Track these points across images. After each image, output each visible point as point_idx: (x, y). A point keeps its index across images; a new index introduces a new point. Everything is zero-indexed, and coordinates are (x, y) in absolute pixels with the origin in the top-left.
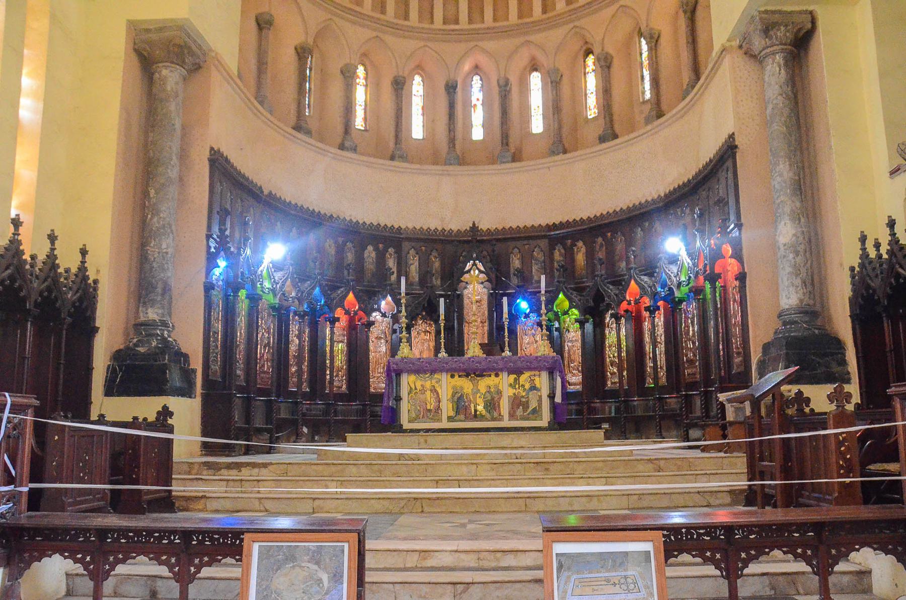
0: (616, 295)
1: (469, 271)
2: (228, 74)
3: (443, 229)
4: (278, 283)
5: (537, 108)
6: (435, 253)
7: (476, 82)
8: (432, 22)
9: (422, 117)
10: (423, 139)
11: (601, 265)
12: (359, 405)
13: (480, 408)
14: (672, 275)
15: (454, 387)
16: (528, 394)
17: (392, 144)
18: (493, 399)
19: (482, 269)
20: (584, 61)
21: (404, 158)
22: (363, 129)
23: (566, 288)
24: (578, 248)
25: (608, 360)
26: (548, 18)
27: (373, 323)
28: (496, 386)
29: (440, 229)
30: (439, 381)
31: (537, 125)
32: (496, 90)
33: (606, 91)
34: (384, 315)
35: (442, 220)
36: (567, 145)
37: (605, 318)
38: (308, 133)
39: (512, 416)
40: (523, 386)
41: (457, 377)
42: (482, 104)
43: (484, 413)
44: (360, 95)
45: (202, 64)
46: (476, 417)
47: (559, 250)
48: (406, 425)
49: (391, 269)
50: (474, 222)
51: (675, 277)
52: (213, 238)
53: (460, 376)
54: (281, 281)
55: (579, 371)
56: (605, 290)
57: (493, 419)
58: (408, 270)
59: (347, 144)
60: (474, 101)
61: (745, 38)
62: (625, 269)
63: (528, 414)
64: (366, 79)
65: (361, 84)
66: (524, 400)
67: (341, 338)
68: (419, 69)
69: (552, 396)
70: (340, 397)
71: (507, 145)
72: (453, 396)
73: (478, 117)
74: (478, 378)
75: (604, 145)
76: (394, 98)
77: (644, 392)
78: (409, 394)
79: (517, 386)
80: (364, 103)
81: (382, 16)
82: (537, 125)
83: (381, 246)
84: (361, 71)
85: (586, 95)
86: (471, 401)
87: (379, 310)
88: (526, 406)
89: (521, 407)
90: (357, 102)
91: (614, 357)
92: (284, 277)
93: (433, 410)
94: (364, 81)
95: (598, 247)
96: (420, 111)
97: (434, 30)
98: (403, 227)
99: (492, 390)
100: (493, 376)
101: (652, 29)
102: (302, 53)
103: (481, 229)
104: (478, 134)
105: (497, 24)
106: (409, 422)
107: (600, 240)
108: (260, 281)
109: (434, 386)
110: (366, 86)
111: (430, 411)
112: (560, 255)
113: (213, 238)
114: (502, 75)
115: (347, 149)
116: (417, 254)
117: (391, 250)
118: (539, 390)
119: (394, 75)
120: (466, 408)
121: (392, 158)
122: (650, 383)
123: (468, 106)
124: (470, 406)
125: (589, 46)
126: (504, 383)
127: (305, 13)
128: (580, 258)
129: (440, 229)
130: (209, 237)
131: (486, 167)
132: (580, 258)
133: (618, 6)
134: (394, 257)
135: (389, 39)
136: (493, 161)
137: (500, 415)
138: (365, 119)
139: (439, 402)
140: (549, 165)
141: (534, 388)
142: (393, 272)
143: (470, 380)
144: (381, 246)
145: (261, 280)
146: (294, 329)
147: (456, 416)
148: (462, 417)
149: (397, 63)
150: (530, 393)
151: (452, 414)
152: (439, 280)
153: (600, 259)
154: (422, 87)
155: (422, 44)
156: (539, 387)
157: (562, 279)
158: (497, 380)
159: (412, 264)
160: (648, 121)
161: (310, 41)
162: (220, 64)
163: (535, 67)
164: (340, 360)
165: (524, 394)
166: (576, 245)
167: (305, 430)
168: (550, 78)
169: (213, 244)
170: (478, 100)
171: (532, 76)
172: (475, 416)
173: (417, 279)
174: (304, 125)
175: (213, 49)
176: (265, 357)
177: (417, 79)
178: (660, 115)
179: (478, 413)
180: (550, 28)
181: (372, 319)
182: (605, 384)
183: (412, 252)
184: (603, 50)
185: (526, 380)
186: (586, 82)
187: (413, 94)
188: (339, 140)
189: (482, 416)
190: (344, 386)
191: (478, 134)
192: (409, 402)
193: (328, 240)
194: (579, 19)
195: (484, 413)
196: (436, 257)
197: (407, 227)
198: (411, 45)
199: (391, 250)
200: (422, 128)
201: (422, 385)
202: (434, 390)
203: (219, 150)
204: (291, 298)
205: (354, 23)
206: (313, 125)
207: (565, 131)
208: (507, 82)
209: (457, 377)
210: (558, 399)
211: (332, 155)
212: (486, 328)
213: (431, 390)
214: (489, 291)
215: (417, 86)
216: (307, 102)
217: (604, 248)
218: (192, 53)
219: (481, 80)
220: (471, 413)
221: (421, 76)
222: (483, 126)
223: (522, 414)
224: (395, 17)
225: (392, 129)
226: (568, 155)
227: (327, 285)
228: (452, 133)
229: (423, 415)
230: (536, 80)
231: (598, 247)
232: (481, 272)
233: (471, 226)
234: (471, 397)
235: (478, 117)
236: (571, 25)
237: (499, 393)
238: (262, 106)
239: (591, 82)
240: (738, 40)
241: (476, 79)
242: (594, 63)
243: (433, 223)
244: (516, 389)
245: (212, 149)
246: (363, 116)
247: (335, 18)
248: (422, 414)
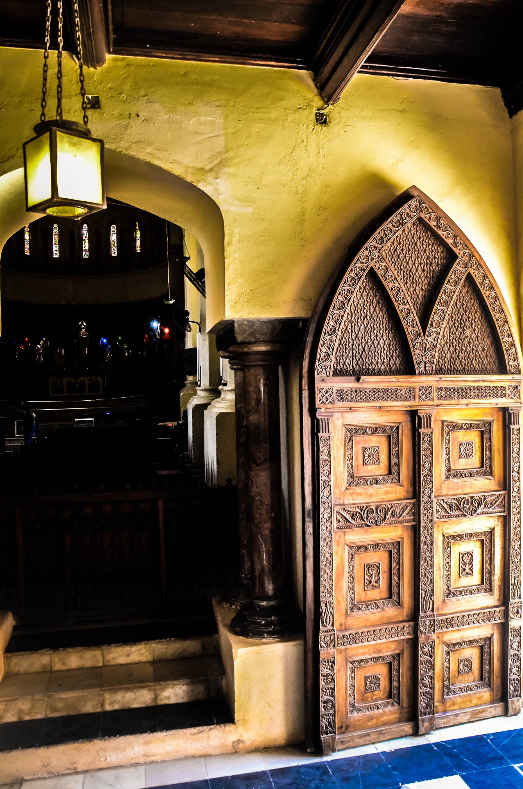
126: (86, 379)
170: (86, 237)
177: (55, 226)
187: (53, 233)
210: (105, 384)
241: (85, 225)
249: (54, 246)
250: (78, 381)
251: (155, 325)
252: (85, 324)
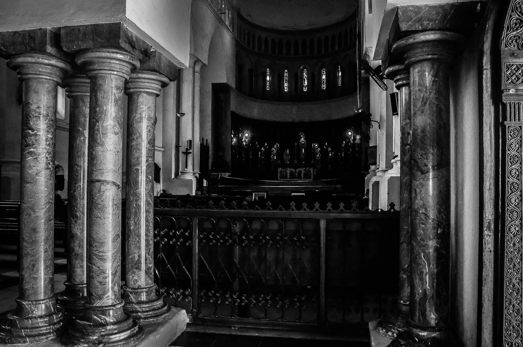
30: (287, 169)
34: (275, 149)
48: (279, 179)
64: (270, 73)
69: (313, 173)
85: (338, 78)
87: (274, 147)
126: (303, 170)
170: (305, 77)
202: (286, 171)
210: (315, 173)
232: (303, 136)
249: (285, 84)
250: (297, 171)
251: (350, 133)
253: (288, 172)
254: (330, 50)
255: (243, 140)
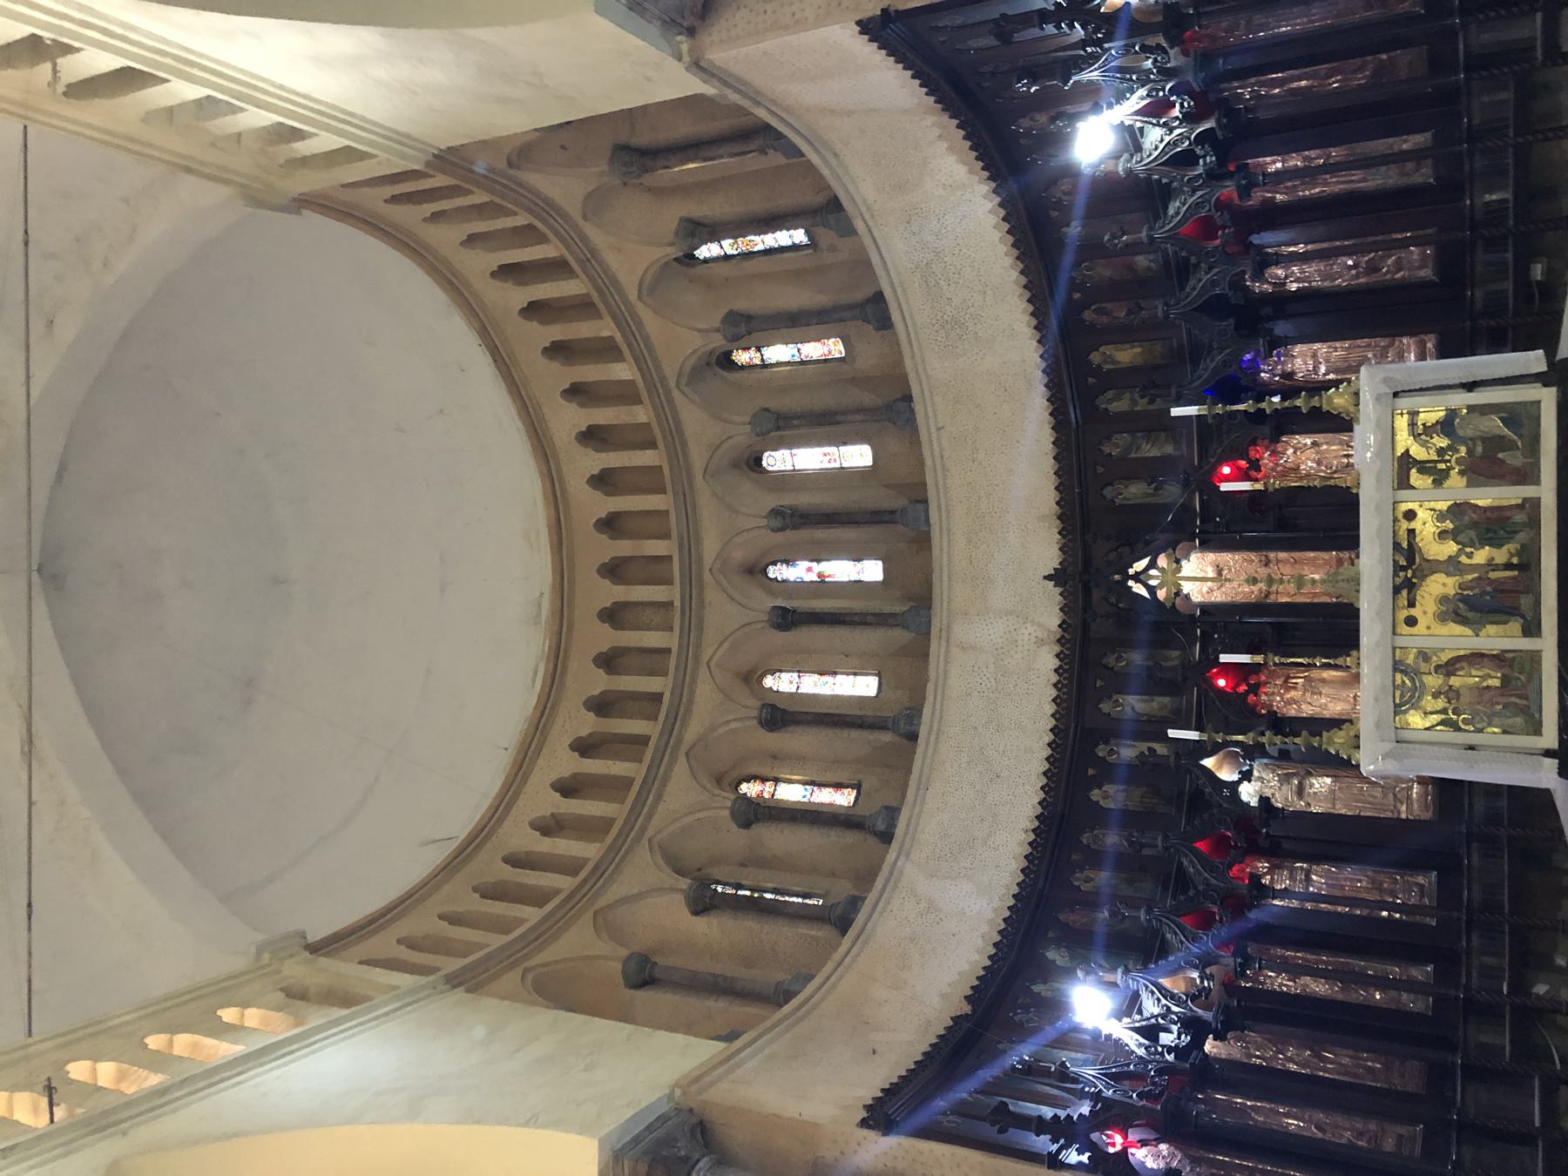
0: (1210, 268)
1: (1151, 590)
2: (721, 1063)
3: (1059, 641)
4: (1168, 1008)
5: (828, 457)
6: (1110, 660)
7: (778, 572)
8: (668, 651)
9: (838, 677)
10: (879, 675)
11: (1141, 309)
12: (1468, 849)
13: (1501, 556)
14: (1167, 139)
15: (1442, 618)
16: (1463, 441)
17: (886, 737)
18: (1474, 525)
19: (1144, 563)
20: (743, 367)
21: (913, 713)
22: (855, 791)
23: (1193, 381)
24: (1106, 362)
25: (1362, 280)
26: (664, 437)
27: (1264, 801)
28: (1441, 517)
29: (1057, 648)
31: (858, 456)
32: (792, 535)
33: (795, 324)
34: (1247, 776)
35: (1040, 642)
36: (899, 396)
37: (1263, 294)
38: (854, 903)
39: (1528, 475)
40: (1441, 451)
41: (1413, 612)
42: (818, 561)
43: (1512, 547)
44: (791, 793)
45: (694, 1120)
46: (1527, 565)
47: (1110, 401)
49: (1142, 753)
50: (1045, 578)
51: (1171, 130)
52: (1059, 1151)
53: (1412, 604)
54: (1164, 1001)
55: (1391, 345)
56: (1200, 295)
57: (1534, 523)
58: (1145, 718)
59: (881, 826)
60: (813, 577)
61: (673, 21)
62: (1152, 257)
63: (1520, 436)
64: (764, 780)
65: (772, 790)
66: (1479, 449)
67: (1300, 876)
68: (752, 679)
70: (1447, 894)
71: (893, 512)
72: (1462, 620)
73: (841, 570)
74: (1417, 560)
75: (895, 317)
76: (799, 729)
77: (1450, 188)
78: (1460, 729)
79: (1442, 466)
80: (808, 787)
81: (652, 744)
82: (858, 456)
83: (1091, 772)
84: (750, 789)
85: (802, 363)
86: (1479, 578)
88: (1495, 443)
89: (1500, 455)
90: (806, 800)
91: (1355, 266)
92: (1153, 993)
93: (1506, 671)
94: (768, 784)
95: (1105, 319)
96: (826, 678)
97: (680, 646)
98: (1052, 722)
99: (1451, 526)
100: (1414, 525)
101: (677, 234)
102: (703, 902)
103: (1060, 564)
104: (872, 571)
105: (674, 534)
106: (1537, 730)
107: (1088, 315)
108: (1162, 1053)
109: (1438, 667)
110: (776, 780)
111: (1505, 680)
112: (1120, 399)
113: (1059, 1151)
114: (765, 522)
115: (892, 825)
116: (1110, 697)
117: (1101, 751)
118: (1452, 414)
119: (758, 726)
120: (1500, 588)
121: (913, 737)
122: (1424, 175)
123: (822, 586)
124: (1496, 580)
125: (713, 361)
127: (635, 891)
128: (1126, 355)
129: (1057, 648)
130: (1054, 1162)
131: (936, 552)
132: (1126, 355)
133: (639, 303)
134: (1117, 745)
135: (693, 730)
136: (923, 541)
137: (1520, 507)
138: (838, 786)
139: (1482, 655)
140: (933, 430)
141: (1446, 426)
142: (1150, 749)
143: (1424, 577)
144: (1091, 772)
145: (1160, 1049)
146: (1279, 982)
147: (1523, 617)
148: (1525, 601)
149: (735, 720)
150: (1461, 433)
151: (1515, 626)
152: (1166, 652)
153: (1130, 312)
154: (783, 675)
155: (703, 671)
156: (1442, 414)
157: (1173, 391)
158: (1422, 514)
159: (1133, 708)
160: (848, 230)
161: (684, 883)
162: (696, 1079)
163: (752, 462)
164: (1356, 880)
165: (1463, 451)
166: (1099, 367)
167: (1541, 989)
168: (769, 432)
169: (1073, 1157)
170: (809, 570)
171: (770, 469)
172: (1520, 567)
173: (1167, 700)
174: (839, 911)
175: (667, 1091)
176: (1346, 1061)
177: (769, 682)
178: (835, 205)
179: (1515, 560)
180: (681, 432)
181: (1254, 802)
182: (1424, 285)
183: (1105, 707)
184: (718, 330)
185: (1424, 444)
186: (779, 364)
187: (794, 690)
188: (872, 842)
189: (1519, 553)
190: (1421, 880)
191: (872, 571)
192: (1480, 731)
193: (1076, 883)
194: (663, 379)
195: (1512, 547)
196: (1119, 659)
197: (1053, 716)
198: (705, 693)
199: (1101, 751)
200: (858, 678)
201: (1436, 696)
202: (1449, 668)
203: (868, 1108)
204: (1202, 982)
205: (659, 797)
206: (843, 889)
207: (868, 399)
208: (776, 513)
209: (1413, 612)
211: (902, 859)
212: (1282, 555)
213: (1449, 674)
214: (1195, 548)
215: (782, 683)
216: (800, 900)
217: (1104, 305)
218: (669, 1141)
219: (774, 563)
220: (1514, 578)
221: (763, 675)
222: (859, 560)
223: (1519, 454)
224: (656, 718)
225: (855, 734)
226: (915, 392)
227: (1174, 897)
228: (870, 619)
229: (1520, 697)
230: (778, 460)
231: (1105, 319)
232: (1152, 565)
233: (1053, 583)
234: (1470, 577)
235: (841, 570)
236: (676, 393)
237: (1457, 510)
238: (796, 994)
239: (778, 353)
240: (679, 38)
241: (773, 572)
242: (746, 349)
243: (1047, 661)
244: (1449, 469)
245: (864, 1123)
246: (831, 790)
247: (650, 832)
248: (1514, 699)
252: (1140, 565)
253: (1457, 638)
254: (641, 414)
255: (1133, 1041)
